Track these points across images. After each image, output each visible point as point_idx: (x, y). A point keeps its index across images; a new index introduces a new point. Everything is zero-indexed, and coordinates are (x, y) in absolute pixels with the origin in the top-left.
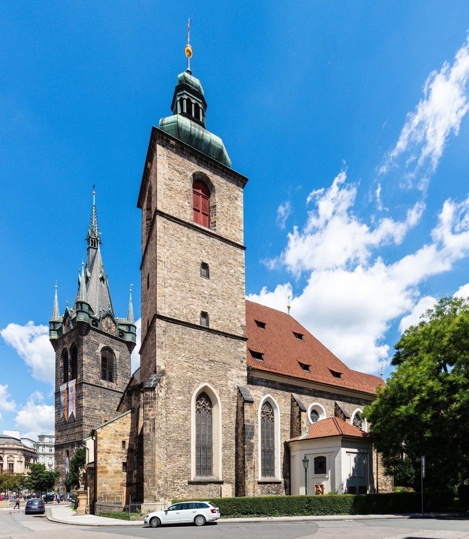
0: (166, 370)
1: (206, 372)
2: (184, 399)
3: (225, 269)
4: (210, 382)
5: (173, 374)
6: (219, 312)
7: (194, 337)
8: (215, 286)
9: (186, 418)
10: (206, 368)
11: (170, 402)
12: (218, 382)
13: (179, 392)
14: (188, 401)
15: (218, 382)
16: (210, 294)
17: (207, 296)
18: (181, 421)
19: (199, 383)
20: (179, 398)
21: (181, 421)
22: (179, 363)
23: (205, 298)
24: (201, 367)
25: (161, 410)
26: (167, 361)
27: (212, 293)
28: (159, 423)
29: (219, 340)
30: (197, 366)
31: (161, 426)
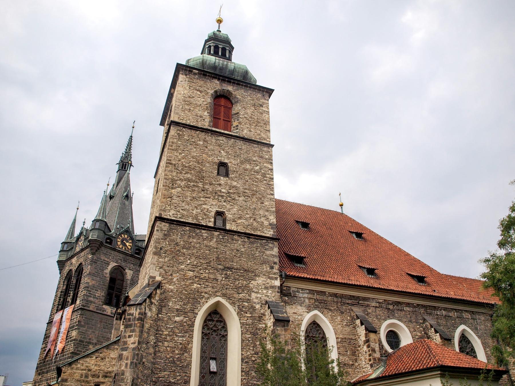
0: (163, 282)
1: (219, 283)
2: (185, 320)
3: (248, 167)
4: (224, 295)
5: (171, 287)
6: (240, 210)
7: (204, 239)
8: (235, 184)
9: (186, 349)
10: (219, 278)
11: (163, 325)
12: (236, 296)
13: (177, 310)
14: (190, 323)
15: (236, 296)
16: (229, 192)
17: (225, 195)
18: (177, 352)
19: (208, 298)
20: (177, 319)
21: (177, 352)
22: (181, 273)
23: (222, 196)
24: (212, 276)
25: (148, 336)
26: (165, 270)
27: (231, 191)
28: (142, 355)
29: (239, 243)
30: (206, 275)
31: (144, 360)
